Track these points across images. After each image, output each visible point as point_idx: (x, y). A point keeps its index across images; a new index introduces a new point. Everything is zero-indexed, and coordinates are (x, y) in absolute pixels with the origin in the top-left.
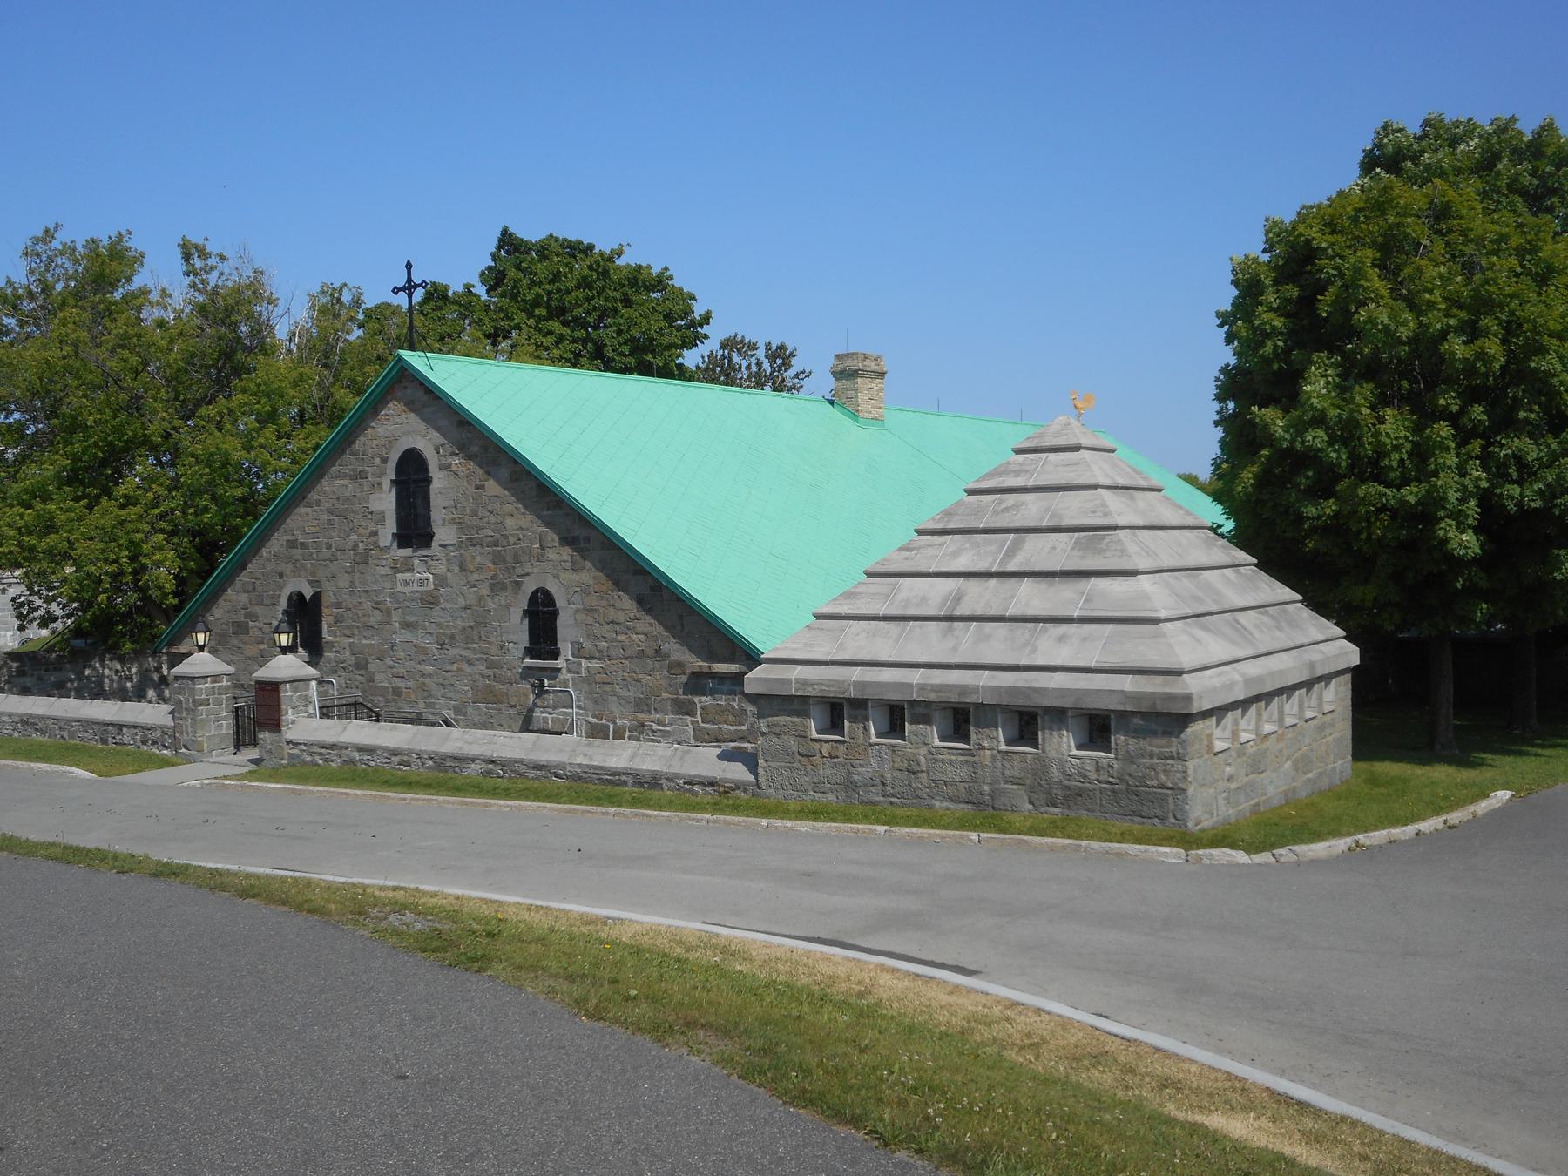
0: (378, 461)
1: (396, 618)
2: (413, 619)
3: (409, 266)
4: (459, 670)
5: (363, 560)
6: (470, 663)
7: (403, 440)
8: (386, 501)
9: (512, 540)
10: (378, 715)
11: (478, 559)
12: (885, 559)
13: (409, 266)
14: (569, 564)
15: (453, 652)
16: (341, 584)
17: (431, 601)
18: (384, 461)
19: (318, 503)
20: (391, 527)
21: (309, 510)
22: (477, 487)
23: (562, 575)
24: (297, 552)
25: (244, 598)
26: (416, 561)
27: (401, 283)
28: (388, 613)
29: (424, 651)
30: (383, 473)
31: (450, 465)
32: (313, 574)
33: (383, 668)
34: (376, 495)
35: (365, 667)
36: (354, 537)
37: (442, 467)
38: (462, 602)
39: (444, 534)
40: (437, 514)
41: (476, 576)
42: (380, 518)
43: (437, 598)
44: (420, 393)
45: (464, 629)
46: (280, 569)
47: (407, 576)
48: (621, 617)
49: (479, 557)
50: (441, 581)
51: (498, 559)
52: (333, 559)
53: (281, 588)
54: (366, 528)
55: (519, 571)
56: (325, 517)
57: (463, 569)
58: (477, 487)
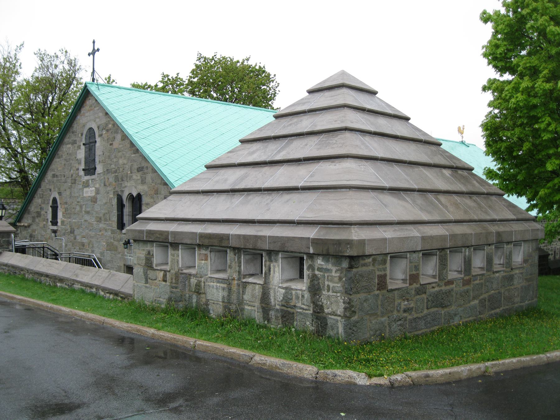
2: (88, 210)
3: (94, 42)
4: (102, 234)
5: (74, 182)
6: (106, 230)
7: (88, 124)
9: (121, 169)
10: (56, 255)
12: (218, 159)
13: (94, 42)
14: (140, 181)
17: (94, 200)
18: (82, 135)
20: (83, 166)
21: (59, 160)
23: (138, 187)
25: (40, 201)
28: (81, 207)
32: (59, 189)
39: (100, 169)
43: (96, 199)
45: (104, 215)
49: (111, 178)
50: (98, 191)
52: (65, 182)
53: (50, 196)
55: (123, 185)
56: (63, 163)
57: (105, 185)
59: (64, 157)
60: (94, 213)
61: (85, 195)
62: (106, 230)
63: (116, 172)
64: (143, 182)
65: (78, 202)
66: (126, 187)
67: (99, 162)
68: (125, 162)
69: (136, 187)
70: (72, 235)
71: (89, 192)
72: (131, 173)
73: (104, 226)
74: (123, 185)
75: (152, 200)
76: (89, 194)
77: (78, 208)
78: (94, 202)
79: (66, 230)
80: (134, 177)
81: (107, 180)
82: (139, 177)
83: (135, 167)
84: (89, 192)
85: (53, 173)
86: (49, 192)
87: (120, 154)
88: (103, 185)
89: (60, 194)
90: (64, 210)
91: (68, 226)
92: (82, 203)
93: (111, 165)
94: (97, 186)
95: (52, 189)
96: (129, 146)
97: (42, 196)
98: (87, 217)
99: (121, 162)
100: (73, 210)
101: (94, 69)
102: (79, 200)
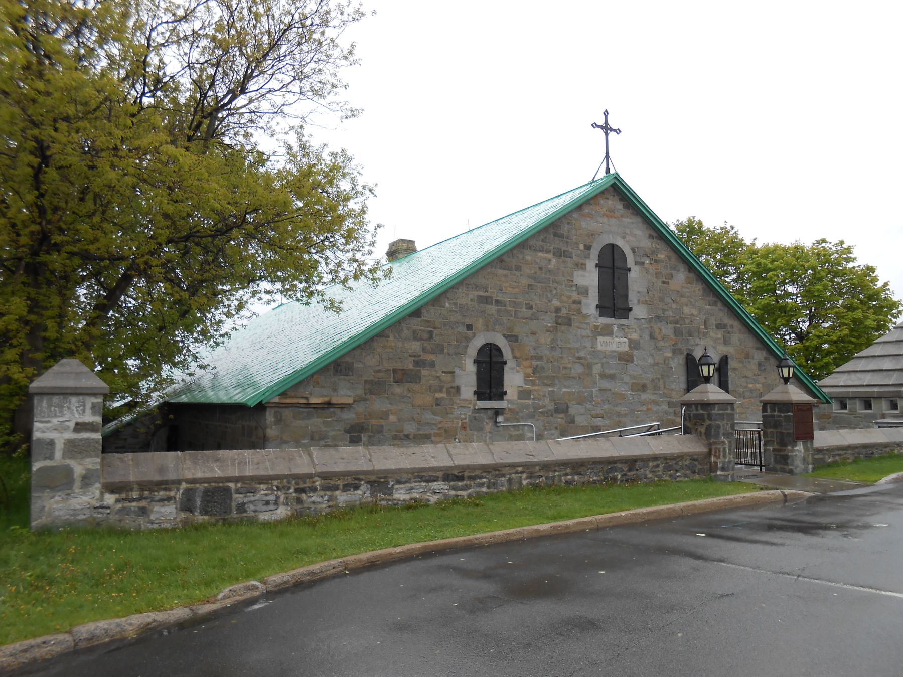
0: (582, 247)
1: (597, 369)
2: (611, 372)
3: (606, 113)
6: (656, 403)
8: (590, 278)
9: (687, 321)
11: (663, 331)
14: (722, 341)
15: (644, 396)
16: (542, 340)
17: (626, 358)
18: (588, 248)
19: (518, 268)
22: (664, 283)
23: (718, 347)
24: (492, 309)
26: (615, 328)
27: (612, 124)
28: (589, 366)
29: (622, 396)
30: (587, 257)
31: (643, 263)
33: (583, 411)
34: (581, 272)
35: (566, 411)
36: (556, 303)
37: (636, 263)
38: (650, 360)
39: (639, 312)
40: (633, 298)
41: (662, 343)
42: (585, 292)
44: (619, 206)
45: (653, 380)
46: (468, 321)
47: (607, 339)
48: (749, 374)
50: (634, 345)
51: (677, 332)
52: (534, 318)
53: (468, 340)
54: (569, 297)
56: (524, 281)
57: (652, 337)
58: (664, 283)
59: (526, 270)
60: (627, 379)
61: (599, 347)
62: (656, 403)
63: (676, 322)
64: (726, 342)
65: (579, 358)
66: (697, 345)
67: (639, 301)
68: (695, 312)
69: (715, 348)
70: (562, 415)
71: (616, 343)
72: (706, 328)
73: (653, 397)
74: (692, 342)
75: (741, 365)
76: (614, 347)
77: (578, 369)
78: (628, 361)
79: (536, 408)
80: (712, 334)
81: (657, 331)
82: (720, 336)
83: (713, 322)
84: (616, 343)
85: (482, 294)
86: (462, 329)
87: (684, 300)
88: (647, 337)
89: (512, 338)
90: (530, 371)
91: (547, 401)
92: (590, 360)
93: (664, 310)
94: (635, 336)
95: (479, 324)
96: (701, 293)
97: (426, 336)
98: (605, 384)
99: (687, 310)
100: (564, 372)
101: (607, 153)
102: (582, 354)
